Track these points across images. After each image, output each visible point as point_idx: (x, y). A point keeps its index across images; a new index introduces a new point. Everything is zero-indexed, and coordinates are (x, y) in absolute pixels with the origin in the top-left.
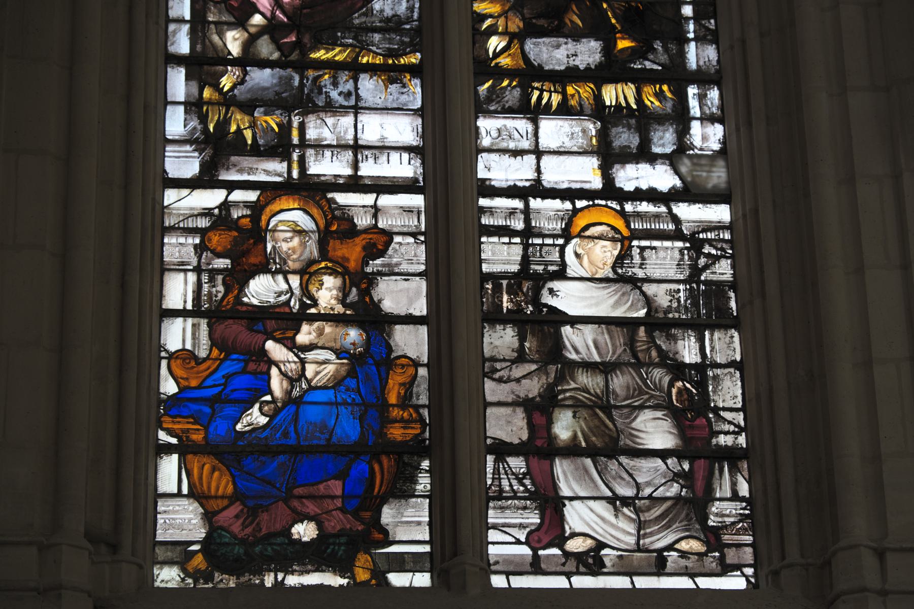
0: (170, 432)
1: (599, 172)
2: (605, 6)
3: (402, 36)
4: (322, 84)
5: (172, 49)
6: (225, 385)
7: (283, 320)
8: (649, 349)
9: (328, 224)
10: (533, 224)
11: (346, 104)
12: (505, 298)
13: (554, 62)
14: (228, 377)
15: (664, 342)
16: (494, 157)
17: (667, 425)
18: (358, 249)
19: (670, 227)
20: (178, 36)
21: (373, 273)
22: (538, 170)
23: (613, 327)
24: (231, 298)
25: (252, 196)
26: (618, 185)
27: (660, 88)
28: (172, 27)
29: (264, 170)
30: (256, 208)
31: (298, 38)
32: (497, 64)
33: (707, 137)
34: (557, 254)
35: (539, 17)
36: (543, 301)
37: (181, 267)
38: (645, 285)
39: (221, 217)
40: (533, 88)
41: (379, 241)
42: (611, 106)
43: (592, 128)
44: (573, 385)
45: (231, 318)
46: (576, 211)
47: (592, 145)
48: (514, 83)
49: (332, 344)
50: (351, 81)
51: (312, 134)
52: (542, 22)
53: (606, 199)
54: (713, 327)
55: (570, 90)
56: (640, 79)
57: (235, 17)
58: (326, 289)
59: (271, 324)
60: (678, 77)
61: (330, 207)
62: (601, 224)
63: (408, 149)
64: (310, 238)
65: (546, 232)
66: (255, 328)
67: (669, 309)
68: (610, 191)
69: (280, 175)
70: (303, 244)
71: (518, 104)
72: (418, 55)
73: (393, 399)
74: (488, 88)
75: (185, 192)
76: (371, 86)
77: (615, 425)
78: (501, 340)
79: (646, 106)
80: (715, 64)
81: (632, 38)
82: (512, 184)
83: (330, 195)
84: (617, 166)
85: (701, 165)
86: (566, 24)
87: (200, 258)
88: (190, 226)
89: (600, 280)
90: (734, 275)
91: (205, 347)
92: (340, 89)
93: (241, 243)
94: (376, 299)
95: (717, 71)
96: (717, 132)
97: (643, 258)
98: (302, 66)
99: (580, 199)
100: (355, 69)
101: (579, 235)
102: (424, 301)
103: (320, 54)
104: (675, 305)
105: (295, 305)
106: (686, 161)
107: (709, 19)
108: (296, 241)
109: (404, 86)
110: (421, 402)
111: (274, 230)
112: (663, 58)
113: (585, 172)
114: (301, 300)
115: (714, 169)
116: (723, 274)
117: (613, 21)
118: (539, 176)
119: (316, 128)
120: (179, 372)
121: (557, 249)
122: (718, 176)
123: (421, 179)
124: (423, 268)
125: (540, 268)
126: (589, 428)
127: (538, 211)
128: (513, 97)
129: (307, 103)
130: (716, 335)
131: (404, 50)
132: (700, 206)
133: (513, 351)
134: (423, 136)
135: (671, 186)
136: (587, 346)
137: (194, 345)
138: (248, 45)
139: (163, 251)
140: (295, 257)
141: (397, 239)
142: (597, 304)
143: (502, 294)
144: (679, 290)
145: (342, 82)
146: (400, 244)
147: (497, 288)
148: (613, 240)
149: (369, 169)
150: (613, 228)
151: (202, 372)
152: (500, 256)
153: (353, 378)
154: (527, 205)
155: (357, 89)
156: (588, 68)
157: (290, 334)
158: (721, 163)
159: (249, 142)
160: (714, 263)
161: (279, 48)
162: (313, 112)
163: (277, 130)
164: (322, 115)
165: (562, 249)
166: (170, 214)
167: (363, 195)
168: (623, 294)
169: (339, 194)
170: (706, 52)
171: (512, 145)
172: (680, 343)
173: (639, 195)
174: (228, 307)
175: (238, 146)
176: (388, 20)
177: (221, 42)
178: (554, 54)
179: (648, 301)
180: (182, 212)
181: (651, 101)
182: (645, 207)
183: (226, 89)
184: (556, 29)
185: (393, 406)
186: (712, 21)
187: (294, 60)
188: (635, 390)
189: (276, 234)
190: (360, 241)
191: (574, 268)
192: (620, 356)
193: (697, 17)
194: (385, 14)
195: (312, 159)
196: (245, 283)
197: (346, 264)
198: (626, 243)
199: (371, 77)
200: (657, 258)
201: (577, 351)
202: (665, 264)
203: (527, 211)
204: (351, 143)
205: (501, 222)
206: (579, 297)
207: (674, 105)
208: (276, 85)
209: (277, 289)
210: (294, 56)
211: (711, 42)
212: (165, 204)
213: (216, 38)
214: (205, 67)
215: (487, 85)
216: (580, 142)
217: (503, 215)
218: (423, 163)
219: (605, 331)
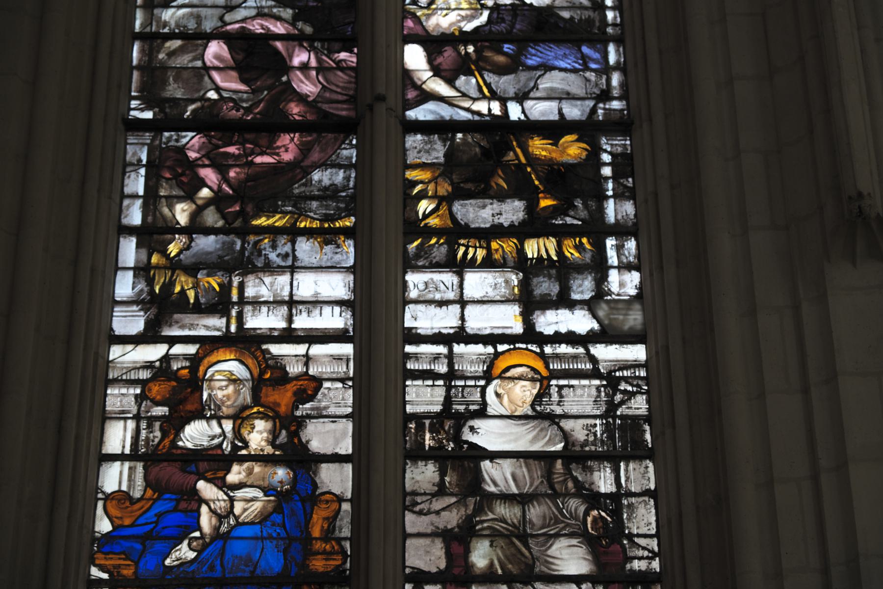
0: (102, 568)
1: (520, 319)
2: (529, 169)
3: (337, 203)
4: (262, 247)
5: (125, 221)
6: (157, 522)
7: (214, 462)
8: (565, 480)
9: (262, 373)
10: (456, 368)
11: (283, 264)
12: (428, 436)
13: (480, 221)
14: (159, 515)
15: (581, 474)
16: (421, 307)
17: (582, 551)
18: (289, 394)
19: (588, 366)
20: (131, 209)
21: (302, 416)
22: (462, 318)
23: (531, 461)
24: (167, 442)
25: (192, 349)
26: (538, 329)
27: (580, 241)
28: (126, 202)
29: (205, 326)
30: (195, 361)
31: (241, 207)
32: (426, 224)
33: (624, 284)
34: (479, 395)
35: (466, 181)
36: (464, 438)
37: (121, 416)
38: (563, 420)
39: (162, 370)
40: (460, 245)
41: (309, 387)
42: (533, 258)
43: (514, 279)
44: (491, 516)
45: (165, 461)
46: (497, 355)
47: (514, 294)
48: (442, 241)
50: (289, 244)
51: (250, 292)
52: (469, 186)
53: (527, 344)
54: (628, 459)
55: (494, 245)
56: (561, 233)
57: (184, 192)
59: (203, 466)
60: (597, 230)
61: (264, 357)
62: (521, 366)
64: (244, 386)
65: (469, 375)
66: (188, 469)
67: (586, 443)
68: (531, 335)
69: (218, 330)
70: (237, 392)
71: (444, 259)
72: (353, 219)
73: (316, 532)
74: (417, 246)
75: (129, 347)
76: (308, 248)
77: (531, 553)
78: (423, 475)
79: (566, 257)
80: (632, 217)
81: (554, 197)
82: (437, 331)
83: (264, 347)
84: (537, 313)
85: (617, 309)
86: (491, 187)
87: (139, 406)
88: (133, 377)
89: (520, 417)
90: (649, 410)
92: (279, 251)
93: (179, 392)
94: (304, 440)
95: (635, 224)
96: (633, 279)
97: (561, 396)
98: (244, 232)
99: (502, 343)
100: (293, 233)
101: (500, 377)
102: (349, 441)
103: (262, 221)
104: (591, 438)
105: (227, 447)
106: (604, 306)
107: (627, 178)
108: (231, 389)
109: (338, 247)
110: (343, 535)
111: (211, 380)
112: (583, 214)
113: (509, 319)
114: (233, 443)
115: (631, 312)
116: (638, 409)
117: (537, 183)
118: (462, 324)
119: (255, 286)
120: (113, 512)
122: (635, 318)
123: (351, 329)
124: (350, 410)
125: (462, 408)
126: (506, 556)
127: (461, 356)
128: (440, 253)
129: (248, 264)
130: (631, 466)
131: (340, 214)
132: (617, 346)
133: (434, 485)
134: (354, 291)
135: (589, 329)
136: (506, 479)
137: (129, 487)
138: (195, 216)
139: (105, 401)
140: (229, 403)
141: (327, 384)
142: (516, 440)
143: (425, 432)
144: (595, 425)
145: (280, 245)
146: (329, 389)
147: (420, 428)
148: (533, 380)
149: (302, 322)
150: (533, 369)
151: (136, 511)
153: (279, 513)
154: (451, 350)
155: (294, 250)
156: (512, 225)
157: (220, 474)
158: (637, 306)
159: (192, 301)
160: (630, 399)
161: (224, 216)
162: (252, 273)
163: (218, 289)
164: (261, 275)
165: (483, 390)
166: (114, 367)
167: (296, 346)
168: (542, 430)
169: (273, 345)
170: (624, 207)
171: (438, 296)
172: (596, 474)
173: (558, 338)
174: (164, 451)
175: (182, 305)
176: (326, 189)
177: (170, 214)
178: (480, 213)
179: (566, 436)
180: (125, 365)
181: (571, 253)
182: (564, 349)
183: (172, 255)
184: (483, 191)
185: (316, 539)
186: (630, 180)
188: (551, 519)
189: (213, 383)
190: (291, 387)
191: (494, 406)
192: (537, 487)
193: (615, 177)
194: (323, 184)
195: (250, 314)
196: (181, 428)
197: (277, 409)
198: (545, 383)
200: (575, 395)
201: (495, 484)
202: (582, 401)
203: (450, 356)
204: (287, 298)
205: (426, 367)
206: (500, 434)
207: (593, 256)
208: (219, 249)
209: (210, 433)
210: (238, 223)
211: (628, 198)
212: (111, 358)
213: (166, 210)
214: (155, 236)
215: (416, 244)
216: (504, 291)
217: (428, 360)
218: (353, 315)
219: (523, 465)
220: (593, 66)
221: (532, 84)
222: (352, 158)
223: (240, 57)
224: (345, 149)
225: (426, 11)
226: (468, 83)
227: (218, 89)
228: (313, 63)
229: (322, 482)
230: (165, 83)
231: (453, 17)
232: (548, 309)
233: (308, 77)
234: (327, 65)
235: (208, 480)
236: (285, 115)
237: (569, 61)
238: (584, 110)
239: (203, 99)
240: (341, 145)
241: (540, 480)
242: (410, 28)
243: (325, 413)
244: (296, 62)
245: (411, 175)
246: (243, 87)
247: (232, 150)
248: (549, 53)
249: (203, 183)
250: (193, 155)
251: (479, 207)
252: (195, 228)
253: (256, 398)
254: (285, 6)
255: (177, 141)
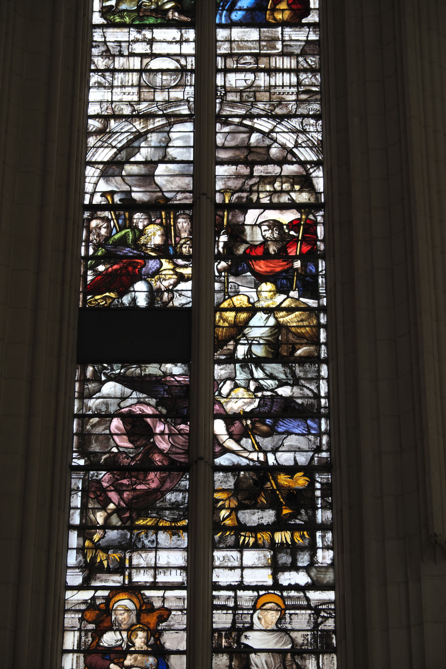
1: (271, 577)
2: (278, 492)
3: (179, 512)
4: (141, 537)
5: (72, 522)
8: (292, 664)
9: (141, 606)
10: (238, 604)
11: (151, 546)
12: (224, 640)
13: (252, 522)
15: (300, 661)
16: (221, 570)
18: (155, 618)
19: (305, 603)
20: (74, 516)
21: (161, 630)
22: (242, 577)
23: (275, 654)
24: (95, 643)
25: (106, 593)
26: (280, 583)
27: (303, 533)
28: (72, 511)
29: (112, 580)
30: (108, 599)
31: (130, 514)
32: (224, 524)
33: (325, 557)
34: (249, 618)
35: (245, 500)
36: (242, 642)
37: (72, 629)
38: (291, 632)
39: (91, 604)
40: (241, 535)
41: (165, 614)
42: (278, 543)
43: (269, 554)
45: (94, 653)
47: (268, 563)
48: (232, 533)
49: (141, 665)
50: (154, 535)
51: (135, 562)
52: (247, 502)
53: (274, 590)
54: (323, 653)
55: (259, 536)
56: (293, 529)
57: (101, 506)
58: (139, 638)
59: (113, 656)
60: (312, 527)
61: (142, 598)
62: (271, 602)
63: (180, 568)
64: (132, 613)
65: (245, 607)
66: (105, 658)
67: (303, 644)
68: (276, 586)
69: (119, 583)
70: (129, 616)
71: (233, 543)
72: (187, 521)
74: (219, 536)
75: (75, 592)
76: (164, 537)
79: (296, 542)
80: (330, 520)
81: (290, 508)
82: (229, 584)
83: (142, 592)
84: (280, 573)
85: (321, 572)
86: (258, 502)
87: (81, 624)
88: (77, 609)
89: (270, 631)
90: (335, 627)
91: (82, 668)
92: (149, 539)
93: (99, 616)
94: (162, 643)
95: (332, 524)
96: (330, 554)
97: (291, 619)
98: (131, 528)
99: (262, 590)
100: (156, 529)
101: (260, 609)
102: (185, 643)
103: (141, 522)
104: (306, 642)
105: (124, 646)
106: (314, 570)
107: (328, 497)
108: (126, 614)
109: (179, 537)
111: (116, 610)
112: (305, 518)
113: (264, 577)
114: (127, 644)
115: (328, 573)
116: (330, 626)
117: (282, 500)
118: (242, 580)
119: (137, 559)
121: (249, 615)
122: (329, 577)
123: (186, 583)
124: (185, 626)
125: (241, 625)
127: (241, 597)
128: (231, 540)
130: (325, 657)
131: (180, 518)
132: (320, 592)
133: (226, 667)
134: (187, 561)
135: (306, 582)
136: (262, 663)
138: (107, 519)
139: (64, 621)
140: (125, 622)
141: (173, 613)
142: (268, 643)
143: (222, 639)
144: (308, 635)
145: (150, 536)
146: (175, 615)
147: (220, 636)
148: (277, 610)
149: (161, 578)
150: (277, 605)
152: (222, 620)
154: (236, 594)
155: (157, 538)
156: (268, 525)
157: (121, 660)
158: (331, 570)
159: (106, 567)
160: (326, 621)
161: (121, 519)
162: (136, 551)
163: (119, 560)
164: (140, 552)
165: (252, 615)
166: (68, 603)
167: (158, 591)
168: (281, 637)
169: (147, 591)
170: (326, 514)
171: (230, 564)
172: (307, 661)
173: (290, 587)
174: (93, 648)
176: (173, 504)
177: (94, 518)
178: (251, 518)
179: (293, 641)
180: (73, 602)
181: (298, 540)
182: (293, 593)
183: (96, 541)
184: (254, 505)
186: (330, 498)
187: (128, 525)
189: (117, 612)
190: (156, 614)
191: (257, 625)
193: (322, 497)
195: (135, 574)
196: (101, 636)
197: (149, 626)
198: (283, 612)
199: (164, 533)
200: (298, 619)
202: (301, 622)
203: (236, 597)
204: (153, 565)
205: (223, 603)
206: (259, 639)
207: (309, 542)
208: (119, 538)
209: (116, 639)
210: (128, 524)
211: (329, 509)
212: (66, 598)
213: (92, 516)
214: (87, 530)
215: (219, 535)
216: (263, 562)
217: (224, 599)
218: (187, 575)
219: (271, 656)
220: (313, 432)
221: (280, 443)
222: (186, 486)
223: (129, 428)
224: (183, 481)
225: (225, 400)
226: (247, 442)
227: (117, 446)
228: (167, 431)
229: (171, 665)
230: (90, 443)
231: (240, 403)
232: (286, 571)
233: (164, 439)
234: (174, 432)
235: (115, 664)
236: (152, 461)
237: (301, 429)
238: (307, 458)
239: (110, 452)
240: (181, 479)
241: (279, 664)
242: (217, 410)
243: (172, 628)
244: (158, 430)
245: (217, 496)
246: (130, 445)
247: (125, 481)
248: (290, 424)
249: (110, 501)
250: (105, 484)
251: (251, 514)
252: (107, 526)
253: (139, 620)
254: (152, 397)
255: (97, 476)
